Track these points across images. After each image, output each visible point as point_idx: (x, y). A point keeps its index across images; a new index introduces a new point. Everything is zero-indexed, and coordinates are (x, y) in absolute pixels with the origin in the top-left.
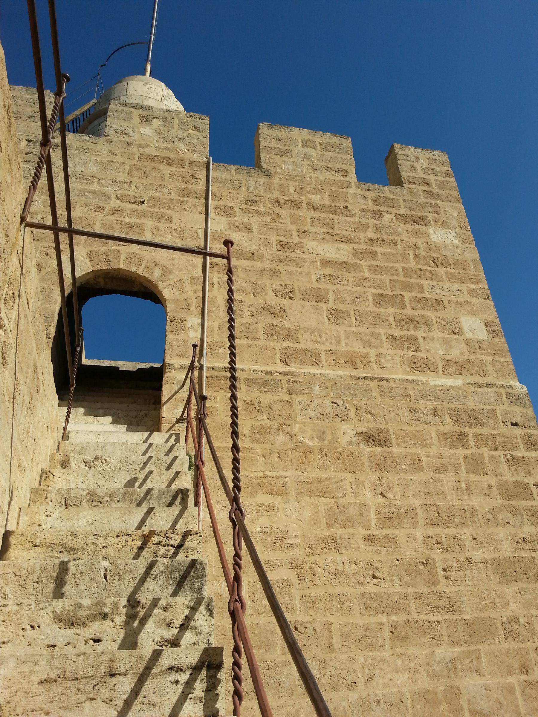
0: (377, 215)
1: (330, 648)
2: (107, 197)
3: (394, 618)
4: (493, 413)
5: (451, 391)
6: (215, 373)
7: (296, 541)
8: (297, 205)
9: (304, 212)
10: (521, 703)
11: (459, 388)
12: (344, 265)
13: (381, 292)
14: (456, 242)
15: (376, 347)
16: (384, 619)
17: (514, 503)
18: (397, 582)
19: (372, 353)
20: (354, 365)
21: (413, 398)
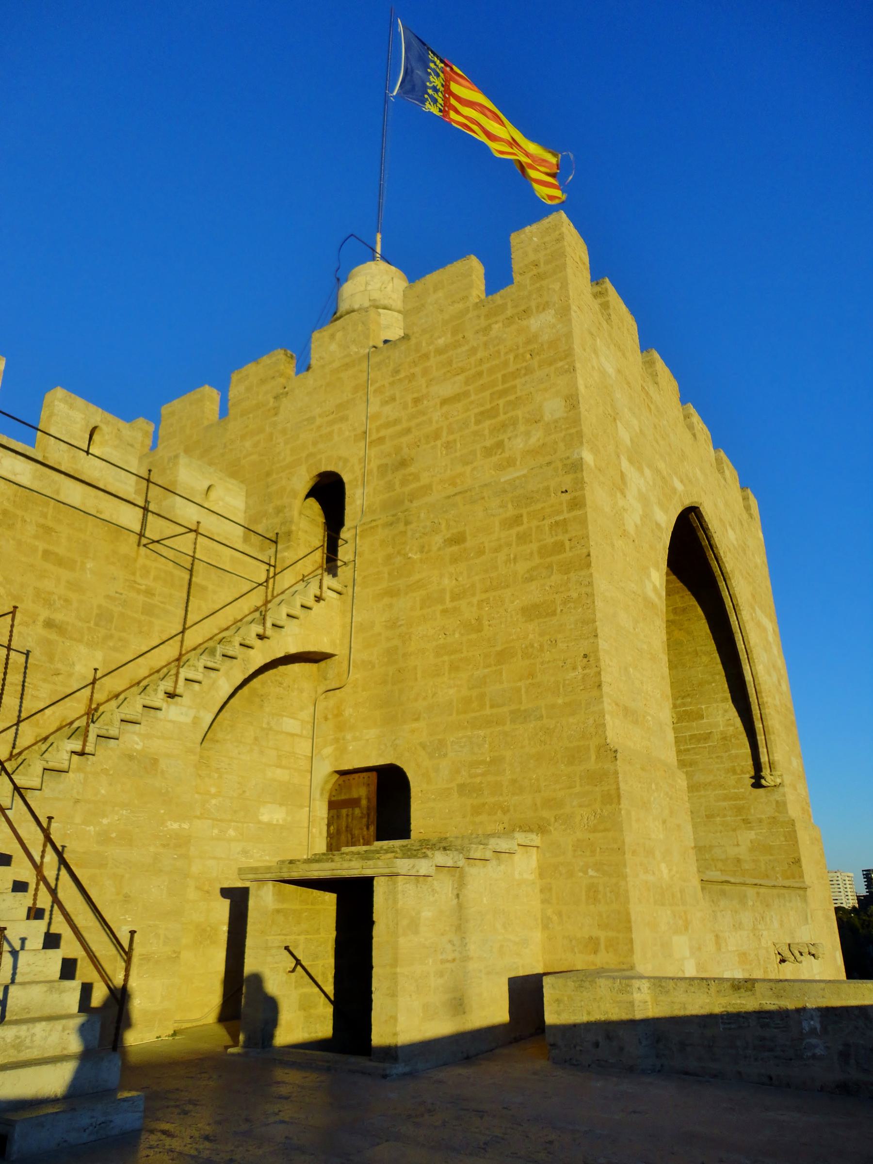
0: (487, 329)
1: (416, 679)
2: (314, 418)
3: (453, 657)
4: (547, 488)
5: (517, 481)
6: (365, 527)
7: (403, 622)
8: (426, 356)
9: (433, 361)
10: (524, 696)
11: (524, 476)
12: (456, 398)
13: (482, 409)
14: (553, 321)
15: (472, 463)
16: (446, 658)
17: (548, 560)
18: (457, 635)
19: (468, 469)
20: (454, 484)
21: (486, 498)
